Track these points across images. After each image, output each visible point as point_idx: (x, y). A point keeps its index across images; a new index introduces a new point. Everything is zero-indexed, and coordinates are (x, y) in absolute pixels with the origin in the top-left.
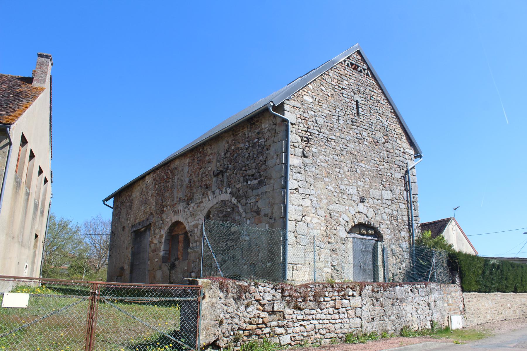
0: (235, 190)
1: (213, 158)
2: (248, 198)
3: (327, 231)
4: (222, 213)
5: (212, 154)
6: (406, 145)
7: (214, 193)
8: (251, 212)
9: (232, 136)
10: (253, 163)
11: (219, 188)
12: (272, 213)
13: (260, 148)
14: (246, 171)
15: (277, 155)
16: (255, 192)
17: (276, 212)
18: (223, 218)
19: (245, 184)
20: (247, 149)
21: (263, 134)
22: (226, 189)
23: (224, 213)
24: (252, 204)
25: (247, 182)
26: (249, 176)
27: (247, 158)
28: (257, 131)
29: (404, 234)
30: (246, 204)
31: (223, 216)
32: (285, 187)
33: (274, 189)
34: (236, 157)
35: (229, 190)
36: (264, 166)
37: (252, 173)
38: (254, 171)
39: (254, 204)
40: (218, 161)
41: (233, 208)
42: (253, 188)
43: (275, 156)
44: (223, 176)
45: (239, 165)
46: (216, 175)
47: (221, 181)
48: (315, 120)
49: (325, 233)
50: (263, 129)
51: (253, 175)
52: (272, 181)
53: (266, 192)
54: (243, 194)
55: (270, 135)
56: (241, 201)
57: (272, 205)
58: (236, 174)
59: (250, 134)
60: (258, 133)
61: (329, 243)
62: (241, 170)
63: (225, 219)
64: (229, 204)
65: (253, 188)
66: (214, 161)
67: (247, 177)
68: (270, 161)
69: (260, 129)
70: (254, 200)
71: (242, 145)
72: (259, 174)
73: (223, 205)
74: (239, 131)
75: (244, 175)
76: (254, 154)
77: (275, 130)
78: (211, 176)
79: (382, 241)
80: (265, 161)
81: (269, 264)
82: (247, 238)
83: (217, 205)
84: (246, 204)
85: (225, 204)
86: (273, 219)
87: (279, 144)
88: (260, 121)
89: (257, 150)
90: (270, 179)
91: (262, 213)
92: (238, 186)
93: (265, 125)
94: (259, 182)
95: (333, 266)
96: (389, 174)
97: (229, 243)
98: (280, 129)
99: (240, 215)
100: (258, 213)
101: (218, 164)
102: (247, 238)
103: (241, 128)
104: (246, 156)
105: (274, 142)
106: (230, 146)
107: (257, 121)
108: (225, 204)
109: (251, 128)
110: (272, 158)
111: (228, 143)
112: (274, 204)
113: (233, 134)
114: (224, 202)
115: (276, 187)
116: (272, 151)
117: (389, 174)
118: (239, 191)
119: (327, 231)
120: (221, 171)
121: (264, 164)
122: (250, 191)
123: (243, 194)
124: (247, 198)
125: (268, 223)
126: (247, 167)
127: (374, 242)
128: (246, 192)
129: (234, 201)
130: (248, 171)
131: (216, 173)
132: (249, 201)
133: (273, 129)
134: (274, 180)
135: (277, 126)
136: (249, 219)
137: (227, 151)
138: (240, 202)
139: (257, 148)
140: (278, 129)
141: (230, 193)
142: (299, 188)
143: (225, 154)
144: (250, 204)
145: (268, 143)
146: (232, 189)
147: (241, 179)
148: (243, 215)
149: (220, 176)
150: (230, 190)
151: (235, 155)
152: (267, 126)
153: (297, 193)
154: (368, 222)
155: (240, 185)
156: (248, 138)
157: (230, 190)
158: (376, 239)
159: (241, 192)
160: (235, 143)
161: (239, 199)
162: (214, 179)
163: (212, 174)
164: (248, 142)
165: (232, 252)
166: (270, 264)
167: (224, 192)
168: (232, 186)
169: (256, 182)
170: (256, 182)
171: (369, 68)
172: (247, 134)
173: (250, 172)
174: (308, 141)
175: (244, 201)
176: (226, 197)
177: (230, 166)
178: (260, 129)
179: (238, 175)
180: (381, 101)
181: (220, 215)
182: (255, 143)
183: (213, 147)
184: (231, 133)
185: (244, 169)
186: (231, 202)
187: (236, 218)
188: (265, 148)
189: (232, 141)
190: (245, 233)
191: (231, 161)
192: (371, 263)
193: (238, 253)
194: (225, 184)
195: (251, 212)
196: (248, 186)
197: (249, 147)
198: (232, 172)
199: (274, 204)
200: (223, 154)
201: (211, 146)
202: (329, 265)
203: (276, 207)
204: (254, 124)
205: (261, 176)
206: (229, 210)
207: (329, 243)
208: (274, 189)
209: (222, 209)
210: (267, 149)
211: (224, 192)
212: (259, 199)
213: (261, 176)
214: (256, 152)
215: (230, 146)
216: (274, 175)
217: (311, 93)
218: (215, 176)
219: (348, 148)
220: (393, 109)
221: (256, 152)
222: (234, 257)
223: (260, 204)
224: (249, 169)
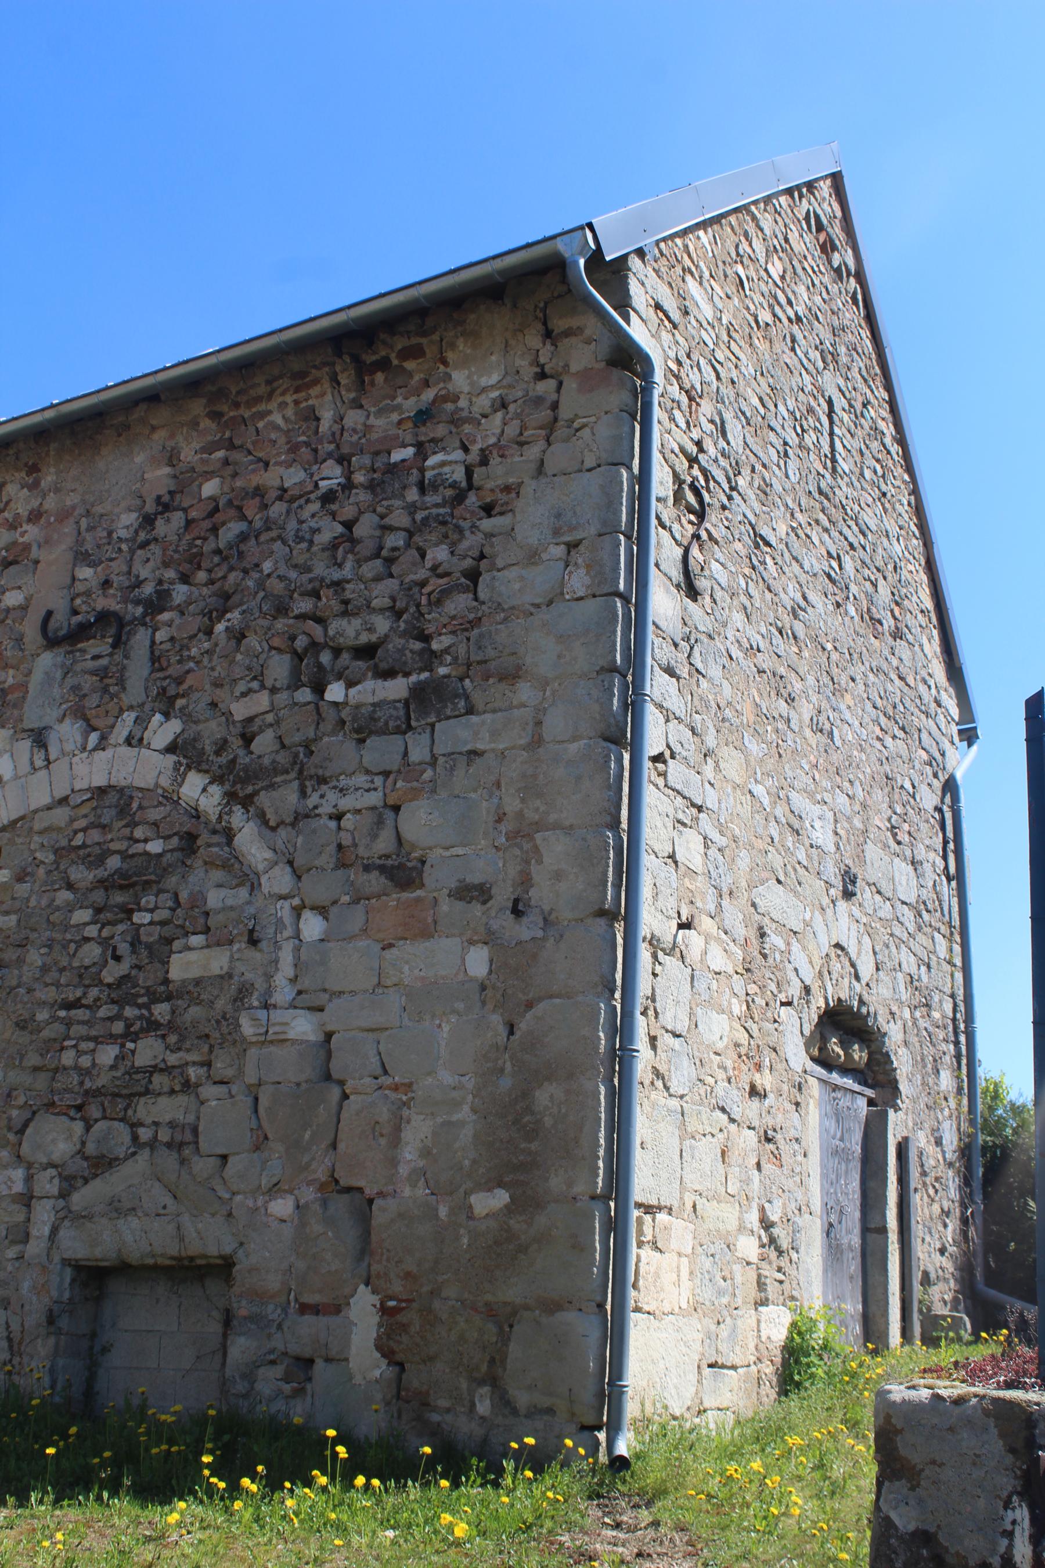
0: (212, 730)
1: (46, 542)
2: (322, 780)
3: (749, 1024)
4: (100, 860)
5: (35, 516)
6: (939, 671)
7: (39, 739)
8: (342, 864)
9: (206, 423)
10: (378, 579)
11: (79, 713)
12: (526, 881)
13: (431, 499)
14: (319, 620)
15: (572, 546)
16: (382, 751)
17: (558, 876)
18: (98, 897)
19: (305, 695)
20: (329, 498)
21: (455, 421)
22: (142, 722)
23: (114, 862)
24: (348, 821)
25: (319, 690)
26: (337, 652)
27: (333, 546)
28: (410, 405)
29: (946, 1081)
30: (300, 817)
31: (103, 884)
32: (621, 732)
33: (537, 742)
34: (243, 537)
35: (163, 731)
36: (459, 604)
37: (364, 638)
38: (382, 625)
39: (368, 818)
40: (82, 557)
41: (189, 842)
42: (364, 727)
43: (559, 551)
44: (115, 645)
45: (261, 585)
46: (64, 637)
47: (102, 674)
48: (720, 414)
49: (742, 1037)
50: (456, 399)
51: (367, 652)
52: (525, 692)
53: (474, 753)
54: (283, 758)
55: (512, 430)
56: (264, 799)
57: (523, 835)
58: (239, 636)
59: (353, 418)
60: (423, 417)
61: (753, 1092)
62: (281, 610)
63: (119, 898)
64: (154, 814)
65: (364, 727)
66: (55, 558)
67: (325, 658)
68: (512, 573)
69: (429, 395)
70: (374, 799)
71: (294, 477)
72: (418, 646)
73: (108, 816)
74: (270, 396)
75: (301, 642)
76: (390, 529)
77: (555, 406)
78: (19, 640)
79: (897, 1109)
80: (473, 576)
81: (490, 1202)
82: (303, 1027)
83: (61, 815)
84: (300, 817)
85: (123, 811)
86: (533, 918)
87: (592, 482)
88: (431, 352)
89: (412, 509)
90: (511, 676)
91: (439, 878)
92: (240, 710)
93: (478, 376)
94: (418, 693)
95: (767, 1224)
96: (908, 785)
97: (147, 1051)
98: (590, 407)
99: (250, 880)
100: (403, 872)
101: (85, 573)
102: (303, 1027)
103: (285, 383)
104: (324, 538)
105: (540, 469)
106: (185, 480)
107: (414, 352)
108: (123, 811)
109: (361, 385)
110: (533, 557)
111: (172, 458)
112: (539, 826)
113: (215, 416)
114: (116, 801)
115: (555, 724)
116: (531, 519)
117: (908, 785)
118: (248, 740)
119: (749, 1024)
120: (104, 617)
121: (466, 590)
122: (338, 749)
123: (283, 758)
124: (311, 777)
125: (489, 938)
126: (329, 601)
127: (862, 1103)
128: (308, 746)
129: (197, 790)
130: (334, 626)
131: (61, 622)
132: (328, 801)
133: (538, 401)
134: (544, 684)
135: (570, 384)
136: (322, 911)
137: (165, 507)
138: (247, 802)
139: (412, 495)
140: (572, 401)
141: (171, 748)
142: (667, 754)
143: (148, 521)
144: (338, 817)
145: (495, 475)
146: (187, 716)
147: (279, 668)
148: (279, 880)
149: (98, 646)
150: (175, 726)
151: (232, 530)
152: (494, 378)
153: (660, 781)
154: (861, 1002)
155: (262, 701)
156: (334, 439)
157: (175, 726)
158: (870, 1093)
159: (264, 743)
160: (226, 462)
161: (241, 786)
162: (47, 660)
163: (30, 629)
164: (343, 460)
165: (163, 1109)
166: (501, 1198)
167: (121, 732)
168: (199, 703)
169: (397, 688)
170: (397, 688)
171: (860, 276)
172: (327, 416)
173: (349, 630)
174: (701, 516)
175: (283, 799)
176: (144, 767)
177: (180, 593)
178: (429, 395)
179: (253, 641)
180: (888, 440)
181: (81, 875)
182: (393, 469)
183: (48, 479)
184: (197, 407)
185: (304, 605)
186: (170, 798)
187: (214, 899)
188: (472, 499)
189: (209, 449)
190: (283, 993)
191: (195, 560)
192: (857, 1214)
193: (221, 1117)
194: (136, 689)
195: (342, 864)
196: (330, 714)
197: (348, 486)
198: (195, 623)
199: (539, 826)
200: (129, 519)
201: (33, 469)
202: (753, 1218)
203: (555, 849)
204: (384, 365)
205: (430, 658)
206: (155, 847)
207: (753, 1092)
208: (537, 742)
209: (95, 835)
210: (488, 510)
211: (121, 732)
212: (415, 794)
213: (430, 658)
214: (399, 518)
215: (185, 480)
216: (541, 649)
217: (707, 274)
218: (52, 642)
219: (809, 610)
220: (915, 492)
221: (399, 518)
222: (184, 1141)
223: (420, 822)
224: (345, 614)
